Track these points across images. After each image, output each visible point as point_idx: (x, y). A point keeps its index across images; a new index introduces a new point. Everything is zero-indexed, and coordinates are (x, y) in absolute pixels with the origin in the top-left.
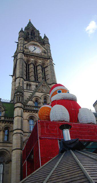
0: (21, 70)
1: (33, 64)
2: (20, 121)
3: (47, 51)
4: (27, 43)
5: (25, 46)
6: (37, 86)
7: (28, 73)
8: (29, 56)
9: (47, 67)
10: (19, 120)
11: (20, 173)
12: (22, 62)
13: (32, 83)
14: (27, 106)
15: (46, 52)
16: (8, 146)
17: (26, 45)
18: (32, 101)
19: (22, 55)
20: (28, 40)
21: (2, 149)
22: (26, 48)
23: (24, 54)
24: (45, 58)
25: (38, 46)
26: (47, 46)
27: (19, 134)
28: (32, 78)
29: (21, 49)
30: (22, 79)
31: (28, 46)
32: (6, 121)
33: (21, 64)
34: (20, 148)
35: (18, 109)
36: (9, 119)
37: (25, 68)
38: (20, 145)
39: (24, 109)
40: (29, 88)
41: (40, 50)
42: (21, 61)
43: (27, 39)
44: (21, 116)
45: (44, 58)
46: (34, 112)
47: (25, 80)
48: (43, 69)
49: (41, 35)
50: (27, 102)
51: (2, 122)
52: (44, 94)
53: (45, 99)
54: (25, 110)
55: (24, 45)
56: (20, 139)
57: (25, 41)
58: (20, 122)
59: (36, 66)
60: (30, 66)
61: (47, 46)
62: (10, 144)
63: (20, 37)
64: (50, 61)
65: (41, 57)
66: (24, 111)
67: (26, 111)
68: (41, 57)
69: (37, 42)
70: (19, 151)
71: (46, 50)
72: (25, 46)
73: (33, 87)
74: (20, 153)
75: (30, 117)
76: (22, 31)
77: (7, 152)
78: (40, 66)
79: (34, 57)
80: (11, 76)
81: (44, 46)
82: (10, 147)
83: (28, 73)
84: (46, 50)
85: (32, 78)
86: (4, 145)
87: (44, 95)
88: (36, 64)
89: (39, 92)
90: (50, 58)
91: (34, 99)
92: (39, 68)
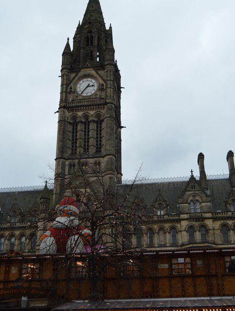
1: (82, 122)
8: (75, 109)
9: (103, 121)
12: (62, 127)
17: (72, 85)
20: (75, 70)
24: (101, 104)
30: (61, 160)
31: (76, 84)
33: (62, 132)
45: (98, 105)
47: (66, 159)
55: (67, 85)
64: (108, 108)
65: (93, 105)
68: (93, 105)
71: (104, 84)
72: (71, 88)
76: (68, 45)
83: (74, 141)
84: (105, 82)
92: (93, 126)
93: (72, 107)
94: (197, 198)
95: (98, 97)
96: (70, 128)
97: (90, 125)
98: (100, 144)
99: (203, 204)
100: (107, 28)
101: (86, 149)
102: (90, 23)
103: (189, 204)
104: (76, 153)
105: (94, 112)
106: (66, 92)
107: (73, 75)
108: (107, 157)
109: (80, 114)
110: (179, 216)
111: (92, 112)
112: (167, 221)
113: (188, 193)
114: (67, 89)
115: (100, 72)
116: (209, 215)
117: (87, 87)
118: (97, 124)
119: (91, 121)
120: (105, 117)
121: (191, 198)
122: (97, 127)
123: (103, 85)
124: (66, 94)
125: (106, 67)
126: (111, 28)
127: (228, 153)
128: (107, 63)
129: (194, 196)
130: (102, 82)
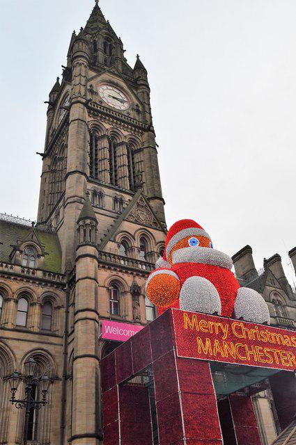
0: (81, 152)
2: (94, 290)
3: (144, 107)
4: (95, 77)
5: (91, 86)
6: (116, 200)
7: (94, 162)
8: (100, 115)
9: (140, 150)
10: (91, 288)
11: (94, 411)
13: (106, 191)
14: (105, 253)
15: (140, 109)
16: (51, 344)
17: (92, 82)
18: (114, 241)
19: (84, 112)
21: (38, 349)
22: (92, 92)
23: (89, 108)
24: (139, 128)
25: (122, 88)
26: (143, 92)
27: (91, 322)
28: (106, 177)
29: (80, 93)
31: (97, 84)
32: (47, 282)
33: (82, 137)
34: (93, 353)
35: (88, 258)
36: (54, 276)
38: (93, 347)
39: (99, 262)
40: (96, 202)
42: (81, 128)
43: (95, 66)
44: (95, 280)
45: (136, 127)
46: (121, 271)
47: (89, 181)
48: (132, 153)
49: (126, 55)
50: (104, 242)
51: (37, 282)
52: (142, 227)
53: (143, 240)
54: (103, 265)
56: (94, 332)
57: (91, 69)
58: (93, 293)
59: (114, 144)
60: (99, 142)
61: (143, 92)
62: (53, 338)
63: (76, 57)
65: (128, 124)
66: (99, 266)
67: (103, 267)
68: (128, 124)
69: (119, 77)
70: (92, 360)
71: (139, 105)
72: (91, 86)
73: (108, 202)
74: (94, 365)
75: (112, 281)
77: (49, 356)
78: (125, 147)
79: (111, 119)
80: (41, 155)
82: (56, 345)
83: (94, 162)
84: (141, 104)
86: (43, 341)
87: (141, 229)
88: (113, 138)
89: (131, 222)
90: (148, 129)
91: (119, 238)
94: (279, 299)
95: (132, 117)
108: (157, 201)
113: (268, 287)
120: (146, 145)
123: (137, 105)
125: (141, 87)
130: (136, 102)
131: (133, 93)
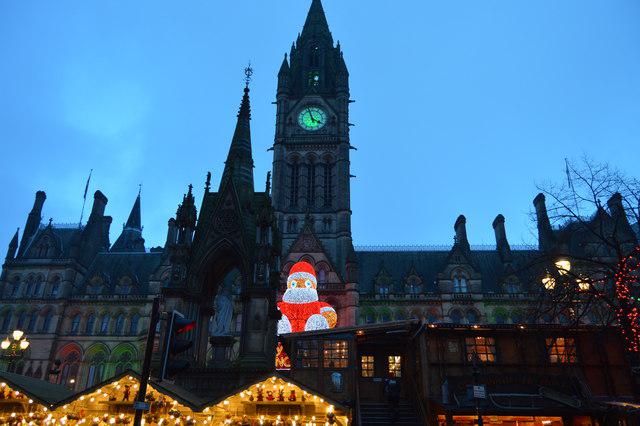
4: (296, 104)
9: (334, 164)
17: (292, 115)
24: (331, 143)
31: (297, 114)
37: (290, 180)
41: (324, 116)
47: (285, 213)
55: (286, 114)
72: (291, 119)
76: (285, 61)
81: (332, 102)
83: (295, 189)
84: (337, 114)
85: (302, 202)
92: (320, 171)
93: (291, 144)
96: (289, 171)
97: (317, 169)
98: (330, 196)
99: (472, 282)
100: (335, 47)
101: (311, 200)
102: (314, 37)
103: (453, 280)
104: (297, 205)
105: (322, 152)
106: (284, 123)
107: (294, 102)
108: (342, 212)
109: (303, 153)
110: (440, 297)
111: (319, 153)
112: (423, 302)
113: (451, 266)
114: (285, 119)
115: (329, 101)
116: (480, 297)
117: (311, 120)
118: (326, 169)
119: (318, 164)
121: (455, 273)
122: (326, 173)
123: (334, 118)
124: (284, 128)
126: (338, 46)
127: (497, 218)
128: (340, 89)
129: (459, 271)
131: (328, 103)
